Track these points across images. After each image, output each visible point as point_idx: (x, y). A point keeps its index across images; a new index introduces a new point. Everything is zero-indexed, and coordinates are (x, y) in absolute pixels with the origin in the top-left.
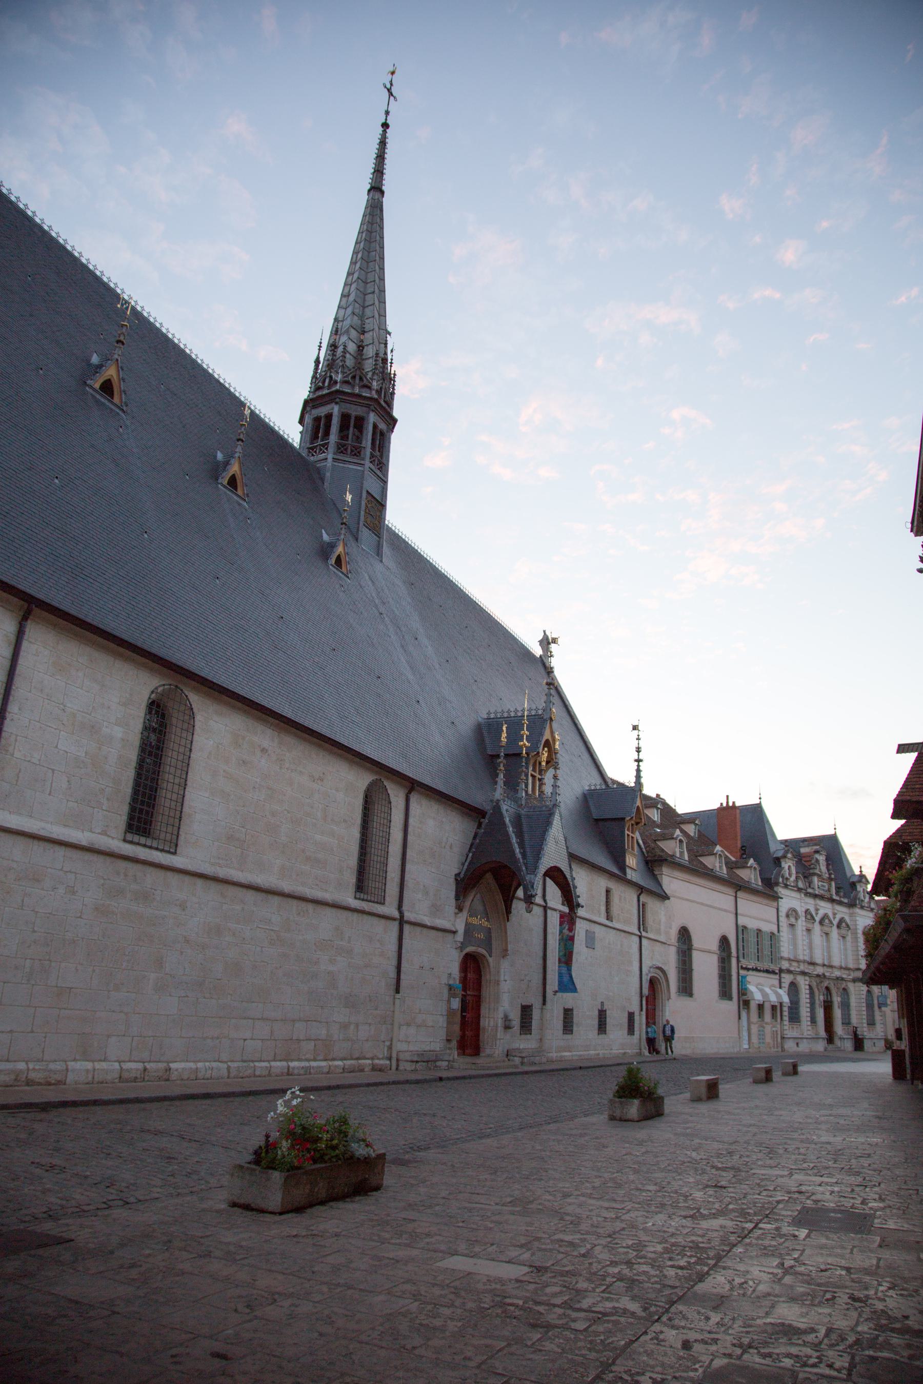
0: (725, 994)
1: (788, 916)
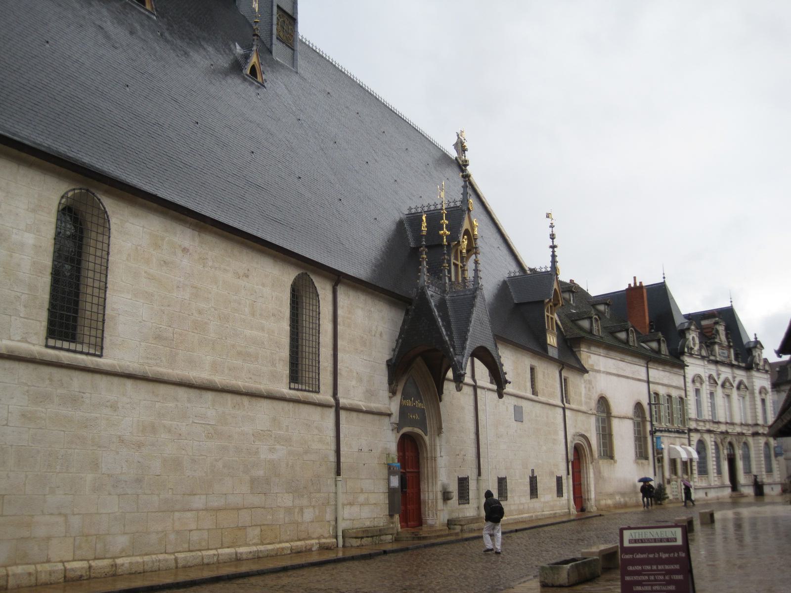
0: (641, 454)
1: (693, 381)
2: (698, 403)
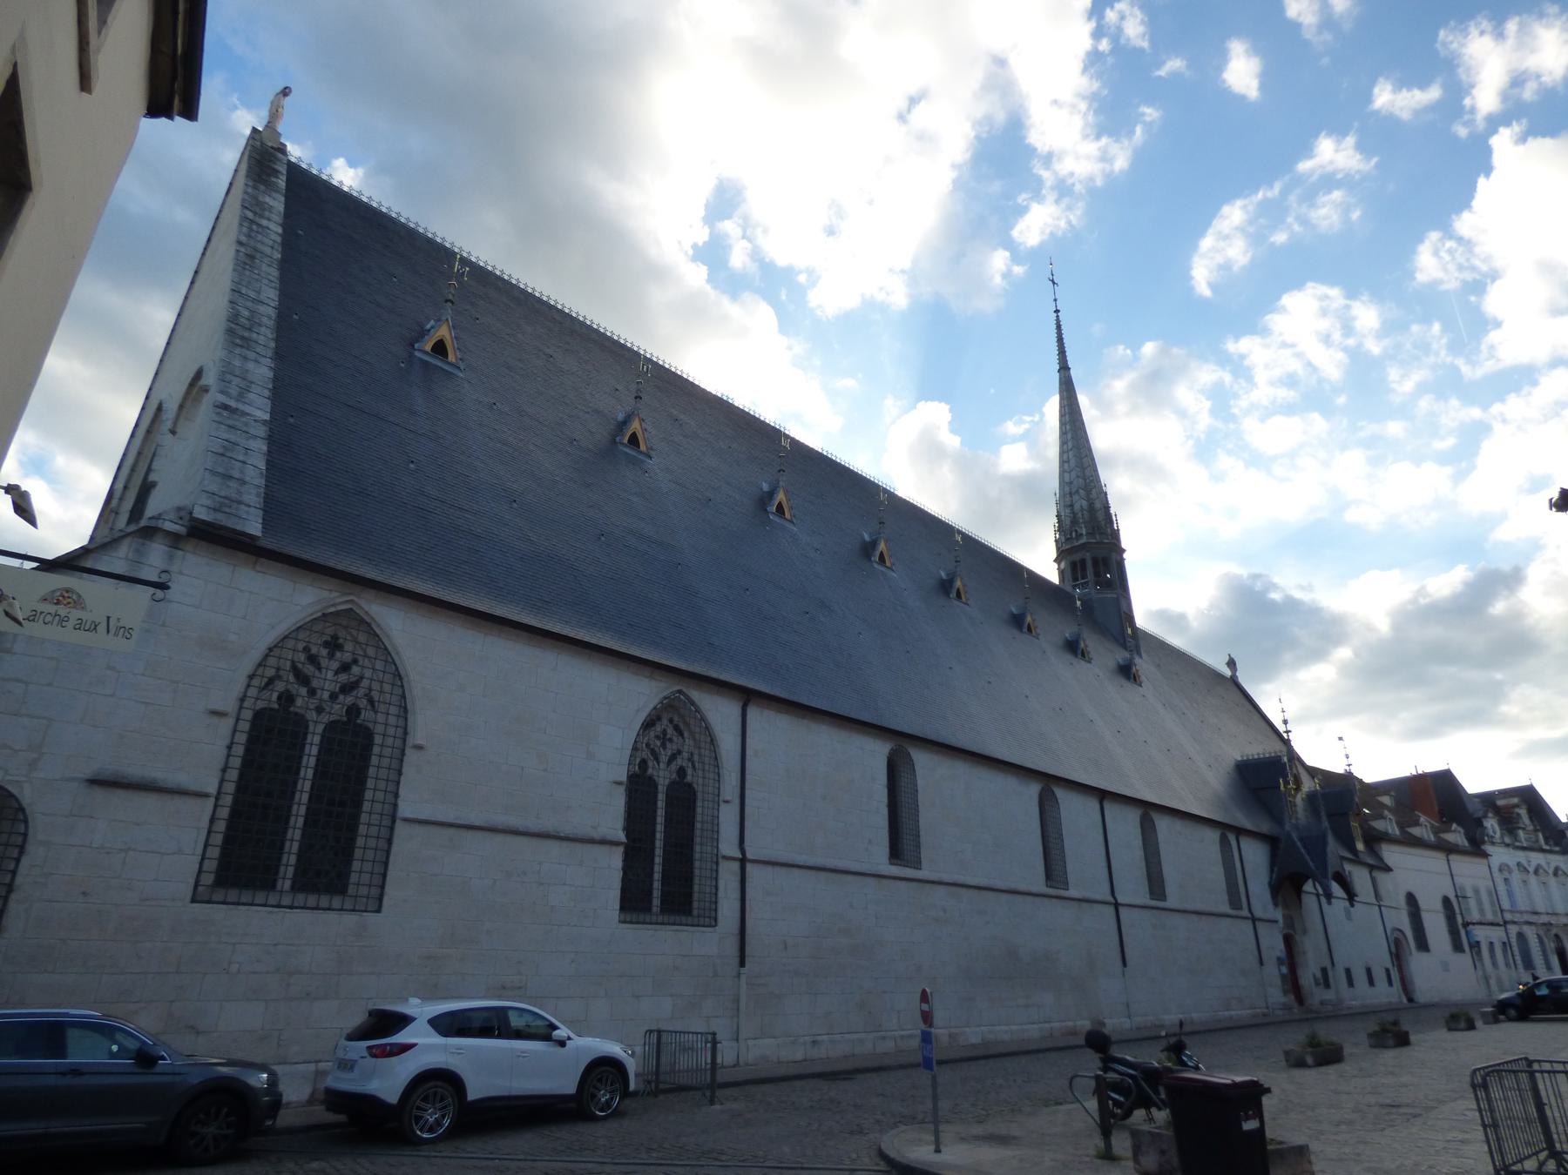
0: (1458, 947)
1: (1500, 870)
2: (1510, 894)
